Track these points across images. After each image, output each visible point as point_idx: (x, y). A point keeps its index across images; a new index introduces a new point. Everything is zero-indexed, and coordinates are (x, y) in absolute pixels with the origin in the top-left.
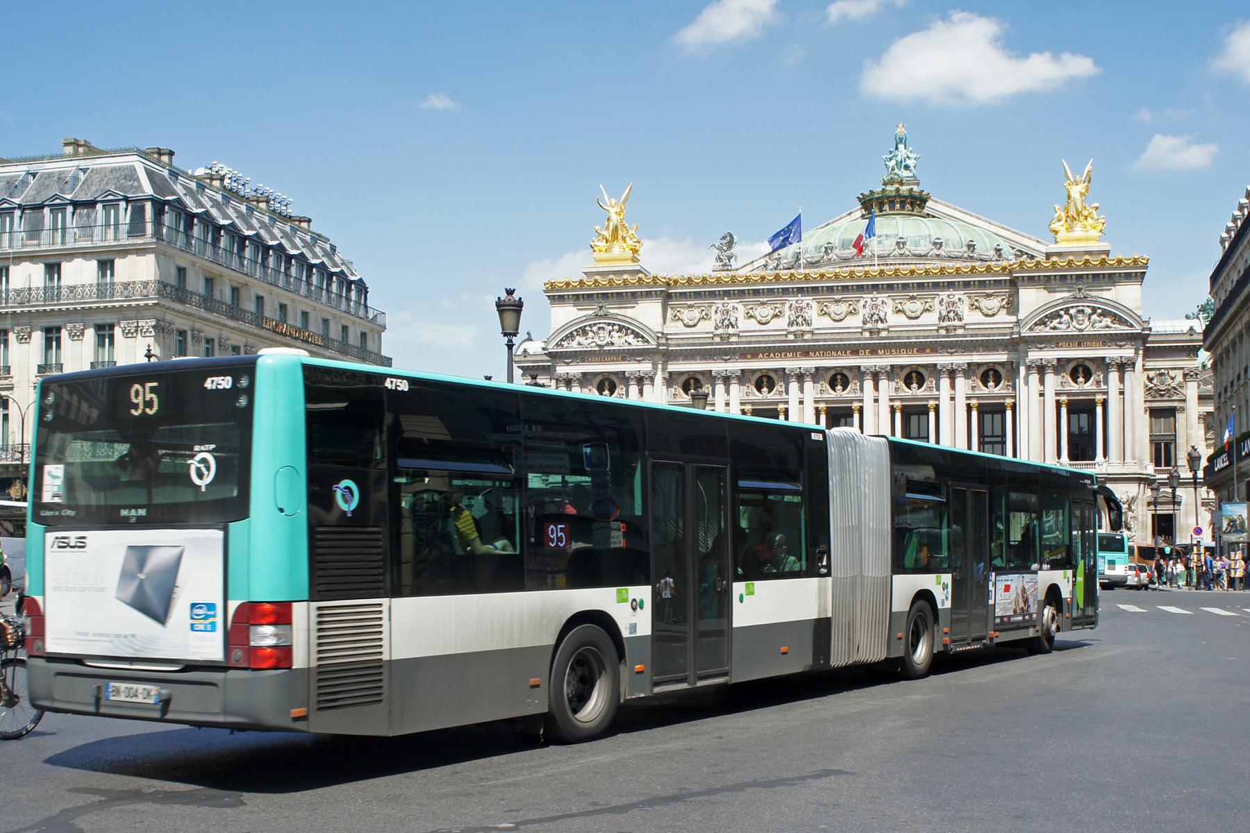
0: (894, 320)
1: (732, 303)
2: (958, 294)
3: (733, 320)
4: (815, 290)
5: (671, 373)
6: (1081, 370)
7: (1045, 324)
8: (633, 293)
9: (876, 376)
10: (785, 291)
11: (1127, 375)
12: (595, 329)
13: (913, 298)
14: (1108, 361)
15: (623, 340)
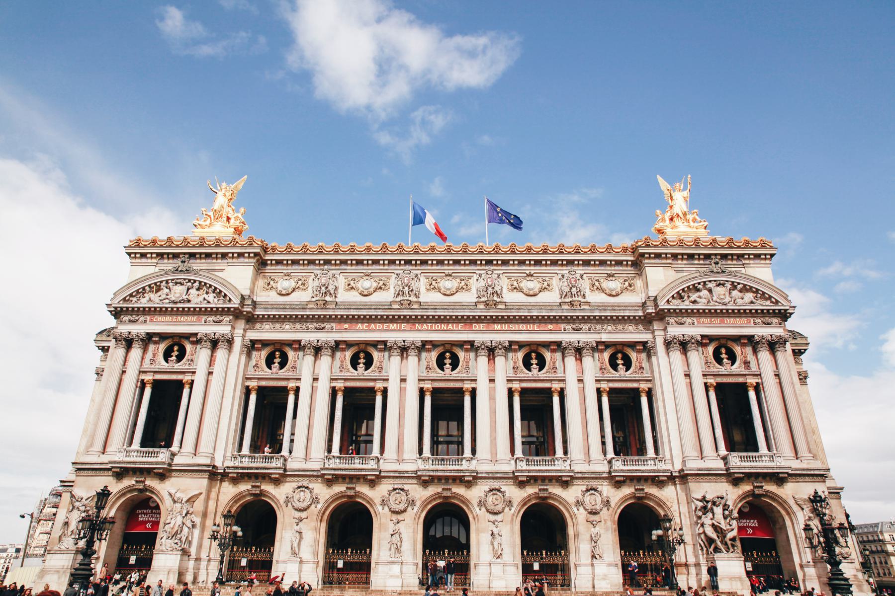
0: (510, 297)
1: (334, 270)
2: (580, 270)
3: (331, 288)
4: (424, 262)
5: (253, 342)
6: (723, 349)
7: (681, 298)
8: (224, 256)
9: (491, 352)
10: (392, 262)
11: (779, 355)
12: (171, 284)
13: (531, 275)
14: (756, 338)
15: (201, 298)
